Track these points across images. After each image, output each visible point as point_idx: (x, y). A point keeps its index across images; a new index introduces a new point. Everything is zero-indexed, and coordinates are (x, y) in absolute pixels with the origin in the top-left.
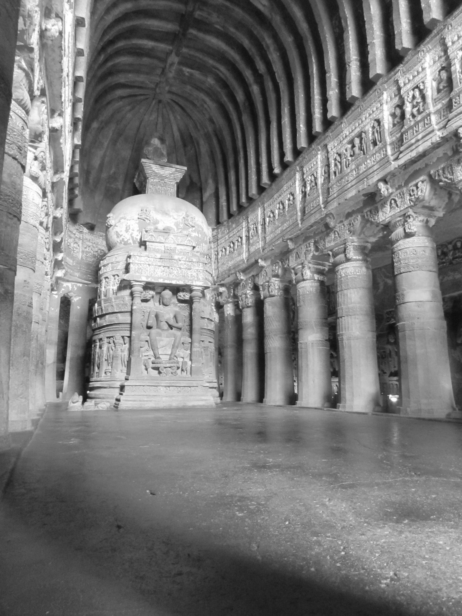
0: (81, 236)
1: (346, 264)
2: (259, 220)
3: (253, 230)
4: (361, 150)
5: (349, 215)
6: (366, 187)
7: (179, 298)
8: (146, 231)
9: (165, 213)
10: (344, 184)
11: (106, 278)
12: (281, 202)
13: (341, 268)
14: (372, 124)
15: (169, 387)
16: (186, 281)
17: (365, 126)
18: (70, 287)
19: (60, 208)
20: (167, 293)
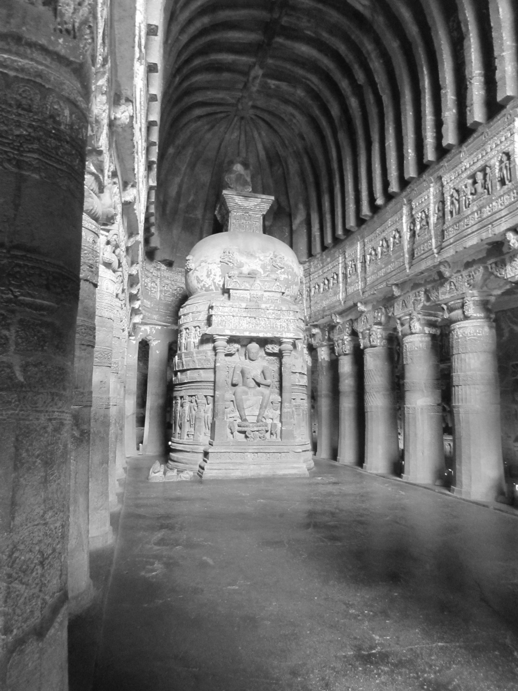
0: (159, 274)
1: (465, 322)
2: (359, 257)
3: (352, 267)
4: (485, 188)
5: (468, 265)
6: (490, 236)
7: (267, 351)
8: (230, 277)
9: (251, 255)
10: (463, 229)
11: (186, 329)
12: (385, 238)
13: (457, 326)
14: (500, 157)
15: (257, 453)
16: (275, 333)
17: (491, 159)
18: (149, 331)
19: (135, 265)
20: (254, 347)
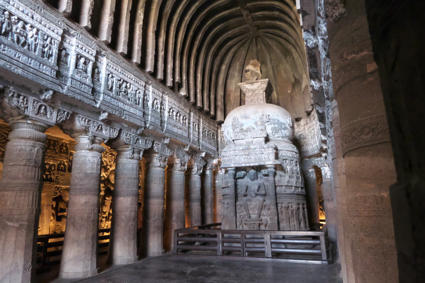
20: (252, 171)
